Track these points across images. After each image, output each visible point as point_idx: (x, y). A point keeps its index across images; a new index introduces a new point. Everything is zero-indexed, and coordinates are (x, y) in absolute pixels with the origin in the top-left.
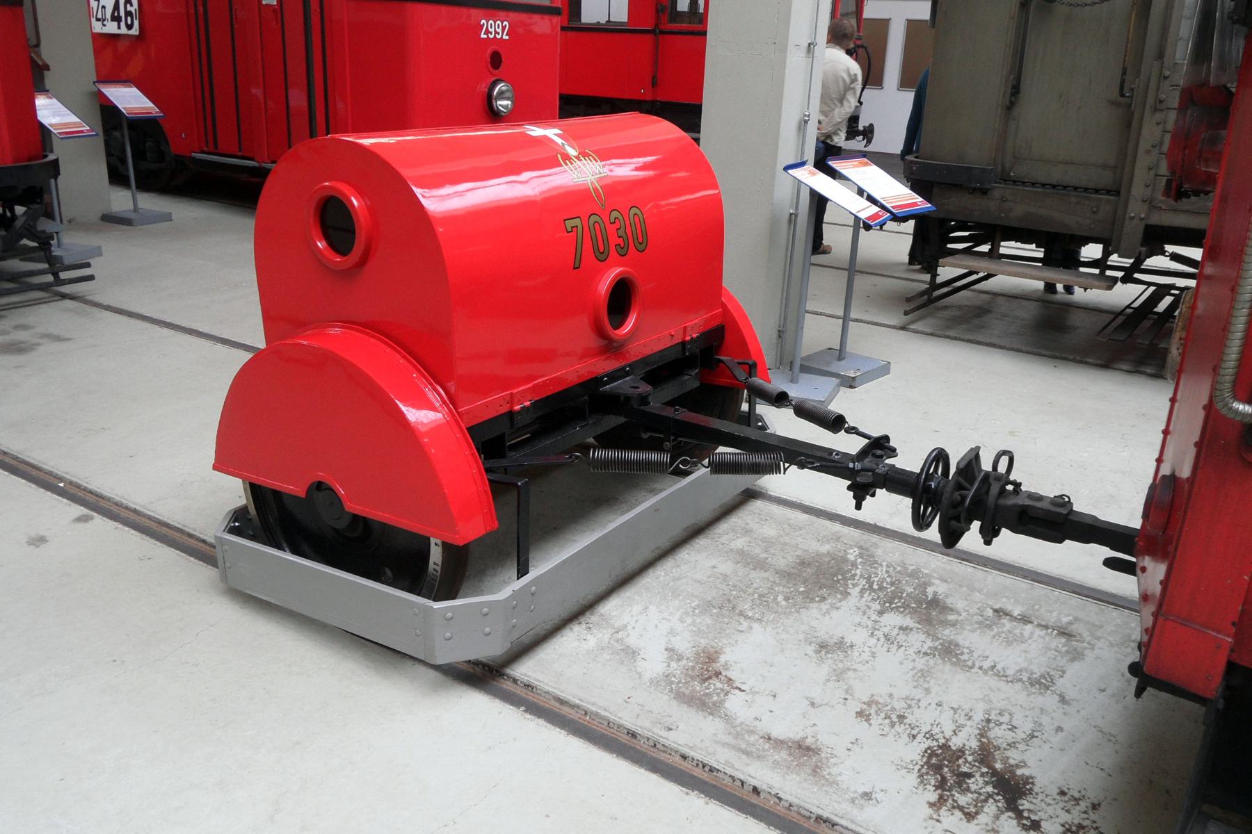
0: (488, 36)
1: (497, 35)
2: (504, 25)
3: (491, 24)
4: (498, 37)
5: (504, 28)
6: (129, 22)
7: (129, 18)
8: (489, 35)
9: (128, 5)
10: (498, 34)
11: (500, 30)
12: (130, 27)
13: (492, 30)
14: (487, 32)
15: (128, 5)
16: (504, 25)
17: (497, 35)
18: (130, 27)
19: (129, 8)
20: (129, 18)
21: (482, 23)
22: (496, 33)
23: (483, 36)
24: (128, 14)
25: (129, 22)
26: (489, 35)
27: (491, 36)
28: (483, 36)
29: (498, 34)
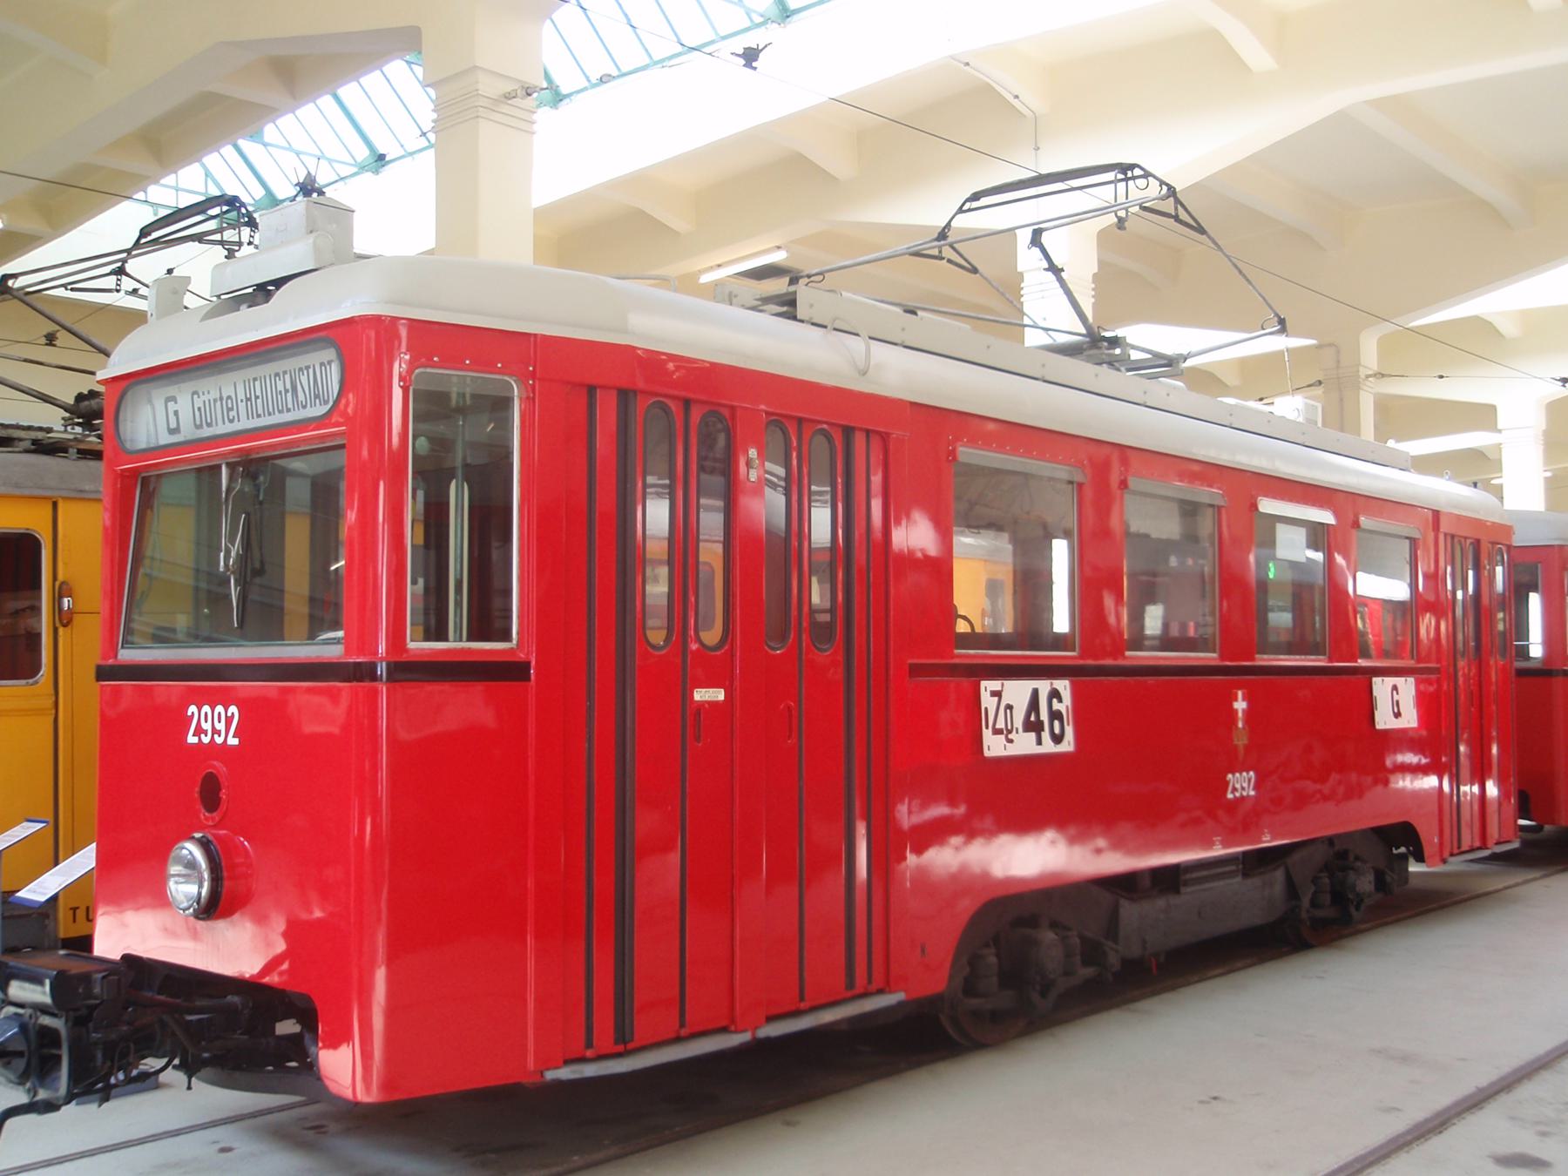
0: (200, 739)
1: (216, 736)
2: (229, 714)
3: (206, 714)
4: (219, 740)
5: (229, 721)
6: (1057, 730)
7: (1056, 723)
8: (203, 736)
9: (1055, 700)
10: (219, 733)
11: (221, 726)
12: (1057, 739)
13: (207, 726)
14: (199, 731)
15: (1055, 700)
16: (229, 714)
17: (216, 736)
18: (1057, 739)
19: (1056, 705)
20: (1056, 723)
21: (189, 713)
22: (215, 731)
23: (192, 739)
24: (1055, 715)
25: (1057, 730)
26: (203, 736)
27: (206, 740)
28: (192, 739)
29: (219, 733)
